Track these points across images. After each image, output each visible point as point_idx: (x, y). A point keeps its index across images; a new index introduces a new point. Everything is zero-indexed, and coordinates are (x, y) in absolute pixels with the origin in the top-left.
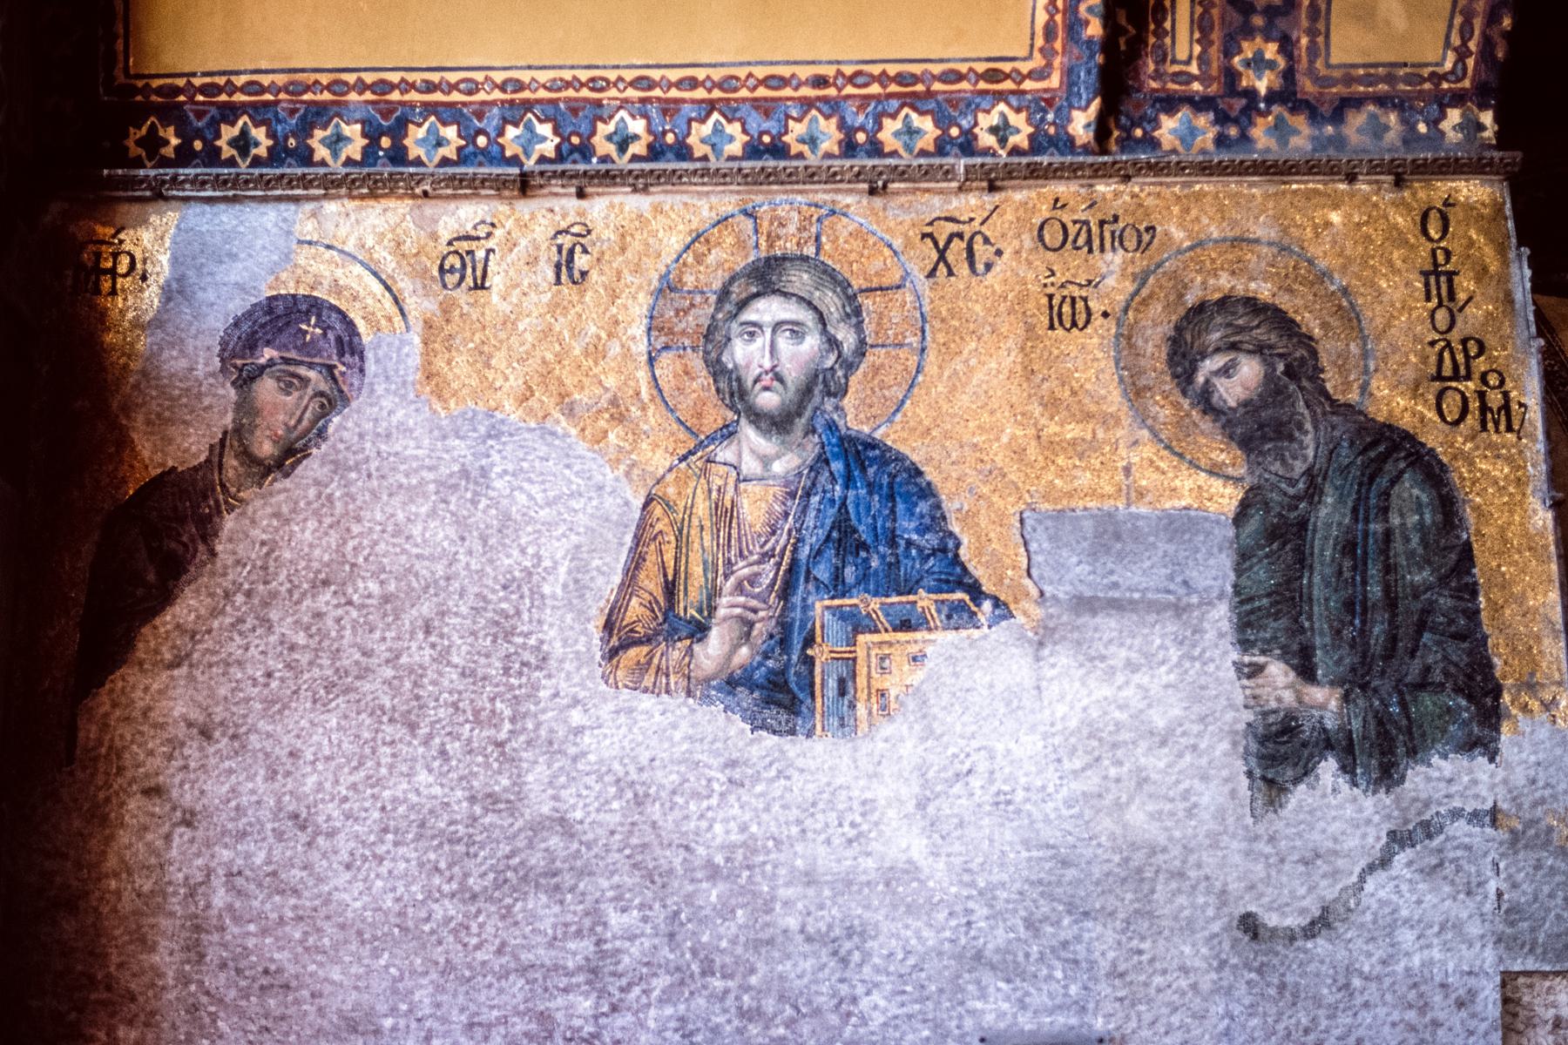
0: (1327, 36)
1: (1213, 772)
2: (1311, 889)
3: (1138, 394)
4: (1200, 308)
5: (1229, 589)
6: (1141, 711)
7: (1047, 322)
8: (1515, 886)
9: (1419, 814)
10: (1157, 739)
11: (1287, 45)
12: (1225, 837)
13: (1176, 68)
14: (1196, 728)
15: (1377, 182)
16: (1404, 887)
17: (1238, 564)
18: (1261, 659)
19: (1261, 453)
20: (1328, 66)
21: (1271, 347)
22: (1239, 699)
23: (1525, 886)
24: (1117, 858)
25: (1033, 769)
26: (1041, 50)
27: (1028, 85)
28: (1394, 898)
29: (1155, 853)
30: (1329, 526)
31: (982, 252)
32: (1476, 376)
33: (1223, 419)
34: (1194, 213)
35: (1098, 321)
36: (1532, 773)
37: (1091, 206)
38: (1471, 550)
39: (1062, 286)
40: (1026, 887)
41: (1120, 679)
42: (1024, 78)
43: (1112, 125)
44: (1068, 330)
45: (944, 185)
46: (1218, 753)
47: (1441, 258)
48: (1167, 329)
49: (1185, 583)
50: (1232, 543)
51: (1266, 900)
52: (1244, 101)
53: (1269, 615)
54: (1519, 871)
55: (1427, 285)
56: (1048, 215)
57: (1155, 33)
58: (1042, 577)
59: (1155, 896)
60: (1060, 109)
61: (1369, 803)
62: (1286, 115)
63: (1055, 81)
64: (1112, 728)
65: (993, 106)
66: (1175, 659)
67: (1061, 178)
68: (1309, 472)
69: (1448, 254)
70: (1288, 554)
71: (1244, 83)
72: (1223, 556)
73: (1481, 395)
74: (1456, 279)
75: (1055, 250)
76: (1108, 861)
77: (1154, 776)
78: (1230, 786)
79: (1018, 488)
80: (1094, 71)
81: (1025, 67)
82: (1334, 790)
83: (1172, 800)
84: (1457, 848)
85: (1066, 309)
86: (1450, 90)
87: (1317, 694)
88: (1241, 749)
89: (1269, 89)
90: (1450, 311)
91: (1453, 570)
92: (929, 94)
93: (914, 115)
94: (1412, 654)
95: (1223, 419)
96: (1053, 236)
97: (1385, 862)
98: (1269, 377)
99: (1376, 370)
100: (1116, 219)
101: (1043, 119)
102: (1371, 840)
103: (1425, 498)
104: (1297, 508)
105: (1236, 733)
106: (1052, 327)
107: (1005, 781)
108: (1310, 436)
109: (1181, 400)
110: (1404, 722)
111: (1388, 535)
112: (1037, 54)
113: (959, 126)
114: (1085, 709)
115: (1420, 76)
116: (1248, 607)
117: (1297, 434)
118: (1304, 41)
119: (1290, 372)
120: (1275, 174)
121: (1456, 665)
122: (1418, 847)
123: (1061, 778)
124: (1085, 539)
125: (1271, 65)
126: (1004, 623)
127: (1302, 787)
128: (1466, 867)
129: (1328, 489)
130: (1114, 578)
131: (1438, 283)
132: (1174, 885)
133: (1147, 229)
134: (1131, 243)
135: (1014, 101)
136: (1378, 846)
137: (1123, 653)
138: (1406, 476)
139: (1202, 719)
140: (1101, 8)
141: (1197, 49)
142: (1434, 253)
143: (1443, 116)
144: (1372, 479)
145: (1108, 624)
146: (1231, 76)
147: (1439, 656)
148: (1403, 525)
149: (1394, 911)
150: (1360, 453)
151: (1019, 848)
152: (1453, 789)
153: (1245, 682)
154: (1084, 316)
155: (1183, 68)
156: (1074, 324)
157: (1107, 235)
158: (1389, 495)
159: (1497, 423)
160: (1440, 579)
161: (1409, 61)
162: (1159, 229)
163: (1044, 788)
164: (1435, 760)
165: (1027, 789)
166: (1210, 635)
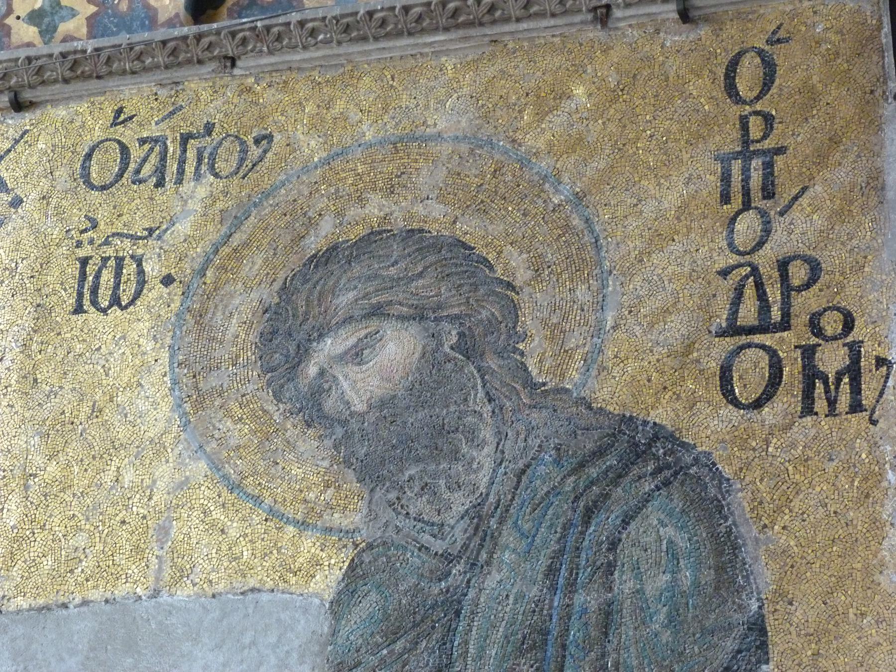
3: (199, 404)
7: (72, 301)
21: (440, 307)
32: (800, 321)
33: (339, 432)
34: (339, 106)
35: (155, 292)
37: (172, 113)
38: (763, 632)
39: (106, 243)
44: (104, 311)
47: (756, 128)
48: (268, 294)
50: (326, 644)
56: (98, 134)
67: (124, 73)
69: (768, 120)
73: (809, 352)
74: (779, 161)
75: (104, 188)
85: (107, 277)
90: (763, 213)
99: (615, 328)
100: (209, 129)
103: (682, 543)
106: (79, 309)
108: (486, 450)
109: (271, 408)
117: (465, 449)
124: (73, 652)
129: (508, 537)
131: (746, 171)
133: (257, 141)
144: (588, 515)
150: (574, 471)
154: (133, 287)
156: (115, 301)
157: (191, 154)
158: (613, 545)
159: (832, 403)
162: (277, 137)
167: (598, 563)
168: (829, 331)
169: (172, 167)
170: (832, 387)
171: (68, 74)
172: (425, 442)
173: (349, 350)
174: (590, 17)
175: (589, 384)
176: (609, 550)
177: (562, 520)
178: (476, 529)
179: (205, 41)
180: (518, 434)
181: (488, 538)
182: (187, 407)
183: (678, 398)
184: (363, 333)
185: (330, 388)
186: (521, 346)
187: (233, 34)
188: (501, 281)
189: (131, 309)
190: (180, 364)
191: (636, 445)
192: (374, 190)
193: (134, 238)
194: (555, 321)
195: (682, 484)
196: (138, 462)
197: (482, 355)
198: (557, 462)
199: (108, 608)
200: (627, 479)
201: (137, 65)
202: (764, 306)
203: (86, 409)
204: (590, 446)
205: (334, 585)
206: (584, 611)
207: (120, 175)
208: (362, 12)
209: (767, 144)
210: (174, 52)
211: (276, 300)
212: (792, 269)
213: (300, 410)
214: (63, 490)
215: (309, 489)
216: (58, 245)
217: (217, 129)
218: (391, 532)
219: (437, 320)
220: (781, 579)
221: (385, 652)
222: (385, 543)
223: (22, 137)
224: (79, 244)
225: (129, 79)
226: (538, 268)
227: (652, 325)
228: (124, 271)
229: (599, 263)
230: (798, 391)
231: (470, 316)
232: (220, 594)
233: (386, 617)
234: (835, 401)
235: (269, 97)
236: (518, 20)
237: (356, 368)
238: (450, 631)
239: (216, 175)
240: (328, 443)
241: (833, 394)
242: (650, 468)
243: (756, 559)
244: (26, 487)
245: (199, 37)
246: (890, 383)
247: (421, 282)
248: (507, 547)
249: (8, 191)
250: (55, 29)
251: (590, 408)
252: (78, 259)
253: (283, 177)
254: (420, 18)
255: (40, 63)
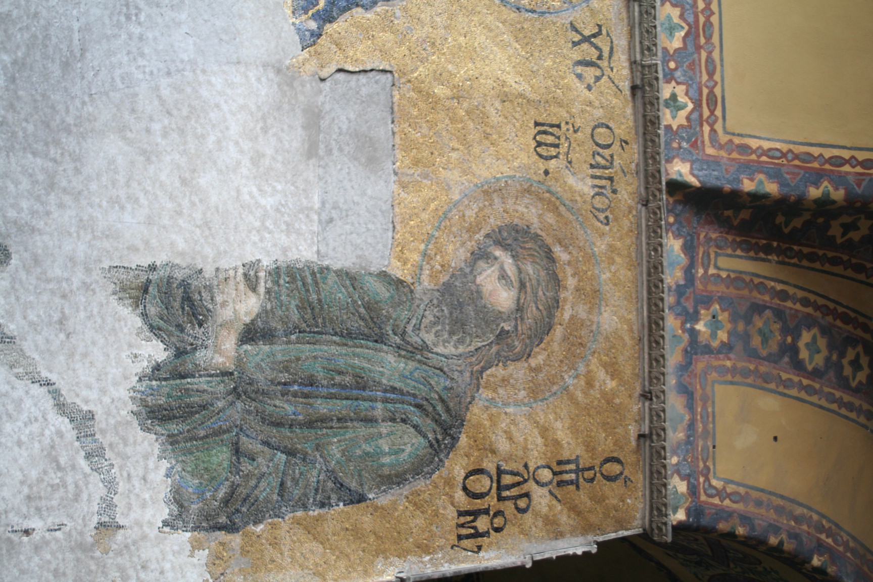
0: (732, 383)
1: (155, 228)
2: (31, 324)
3: (486, 193)
4: (550, 257)
5: (326, 263)
6: (215, 163)
7: (541, 120)
8: (37, 549)
9: (111, 445)
10: (187, 175)
11: (727, 348)
12: (89, 237)
13: (712, 256)
14: (198, 216)
15: (643, 419)
16: (35, 428)
17: (347, 274)
18: (262, 289)
19: (440, 302)
20: (713, 382)
21: (522, 319)
22: (225, 263)
23: (36, 559)
24: (70, 120)
25: (161, 47)
26: (731, 141)
27: (706, 129)
28: (24, 417)
29: (75, 161)
30: (381, 363)
31: (590, 73)
32: (502, 506)
33: (468, 270)
34: (618, 260)
35: (542, 165)
36: (153, 565)
37: (623, 172)
38: (359, 501)
39: (567, 138)
40: (42, 22)
41: (246, 145)
42: (711, 126)
43: (676, 198)
44: (535, 138)
45: (638, 49)
46: (174, 237)
47: (589, 474)
48: (536, 227)
49: (331, 220)
50: (365, 269)
51: (23, 275)
52: (691, 311)
53: (301, 300)
54: (53, 553)
55: (568, 462)
56: (617, 131)
57: (734, 240)
58: (336, 82)
59: (30, 156)
60: (690, 153)
61: (123, 393)
62: (682, 345)
63: (710, 151)
64: (199, 131)
65: (691, 99)
66: (263, 202)
67: (645, 147)
68: (424, 347)
69: (592, 480)
70: (355, 324)
71: (702, 312)
72: (354, 260)
73: (486, 512)
75: (592, 136)
76: (67, 111)
77: (152, 169)
78: (141, 247)
79: (412, 71)
80: (719, 183)
81: (718, 126)
82: (136, 357)
83: (128, 185)
84: (77, 486)
85: (550, 139)
86: (699, 483)
87: (230, 342)
88: (177, 261)
89: (699, 331)
90: (551, 482)
91: (342, 485)
92: (698, 48)
93: (683, 33)
94: (266, 443)
95: (468, 270)
96: (602, 135)
97: (61, 407)
98: (499, 316)
99: (506, 413)
100: (614, 192)
101: (682, 138)
102: (85, 393)
104: (395, 334)
105: (193, 258)
106: (537, 124)
107: (149, 16)
108: (453, 349)
109: (483, 232)
110: (202, 433)
111: (370, 421)
112: (728, 137)
113: (676, 69)
114: (217, 106)
115: (707, 459)
116: (309, 280)
117: (455, 338)
118: (728, 364)
119: (502, 335)
120: (650, 329)
121: (256, 486)
122: (77, 444)
123: (152, 73)
125: (714, 335)
126: (297, 37)
127: (139, 322)
128: (57, 495)
129: (412, 365)
130: (336, 152)
131: (571, 471)
132: (41, 177)
133: (607, 218)
134: (599, 202)
135: (695, 116)
136: (78, 401)
137: (269, 152)
138: (421, 440)
139: (207, 224)
140: (762, 192)
141: (724, 275)
142: (591, 468)
143: (682, 479)
144: (418, 406)
145: (295, 139)
146: (707, 302)
147: (264, 469)
148: (380, 435)
149: (10, 416)
150: (440, 398)
151: (83, 20)
152: (136, 482)
153: (241, 271)
154: (545, 154)
155: (712, 262)
158: (404, 421)
159: (462, 526)
160: (333, 471)
161: (717, 449)
162: (607, 228)
163: (142, 55)
164: (165, 464)
165: (141, 38)
166: (284, 240)
167: (396, 414)
168: (496, 520)
169: (598, 172)
170: (469, 525)
171: (648, 118)
172: (460, 316)
173: (507, 274)
174: (647, 389)
175: (481, 402)
176: (402, 419)
177: (418, 393)
178: (416, 348)
179: (657, 193)
180: (459, 366)
181: (411, 355)
182: (486, 187)
183: (470, 448)
184: (513, 279)
185: (488, 263)
186: (501, 364)
187: (659, 208)
188: (531, 351)
189: (535, 153)
190: (506, 182)
191: (450, 429)
192: (579, 281)
193: (568, 153)
194: (511, 381)
195: (431, 454)
196: (461, 160)
197: (498, 344)
198: (446, 388)
199: (390, 146)
200: (435, 427)
201: (649, 155)
202: (509, 487)
203: (488, 130)
204: (451, 405)
205: (393, 273)
206: (373, 408)
207: (598, 145)
208: (663, 277)
209: (581, 480)
210: (653, 176)
211: (532, 231)
212: (525, 499)
213: (480, 249)
214: (450, 119)
215: (442, 257)
216: (567, 112)
217: (614, 196)
218: (417, 302)
219: (516, 319)
220: (383, 509)
221: (360, 303)
222: (413, 299)
223: (619, 90)
224: (567, 123)
225: (641, 149)
226: (537, 370)
227: (505, 432)
228: (552, 149)
229: (535, 401)
230: (469, 508)
231: (516, 336)
232: (393, 209)
233: (376, 303)
234: (464, 527)
235: (626, 223)
236: (650, 354)
237: (497, 277)
238: (367, 337)
239: (593, 197)
240: (463, 265)
241: (466, 526)
242: (440, 437)
243: (393, 495)
244: (453, 98)
245: (660, 190)
246: (470, 553)
247: (534, 309)
248: (406, 365)
249: (595, 82)
250: (667, 107)
251: (470, 403)
252: (560, 123)
253: (589, 232)
254: (656, 305)
255: (656, 104)
